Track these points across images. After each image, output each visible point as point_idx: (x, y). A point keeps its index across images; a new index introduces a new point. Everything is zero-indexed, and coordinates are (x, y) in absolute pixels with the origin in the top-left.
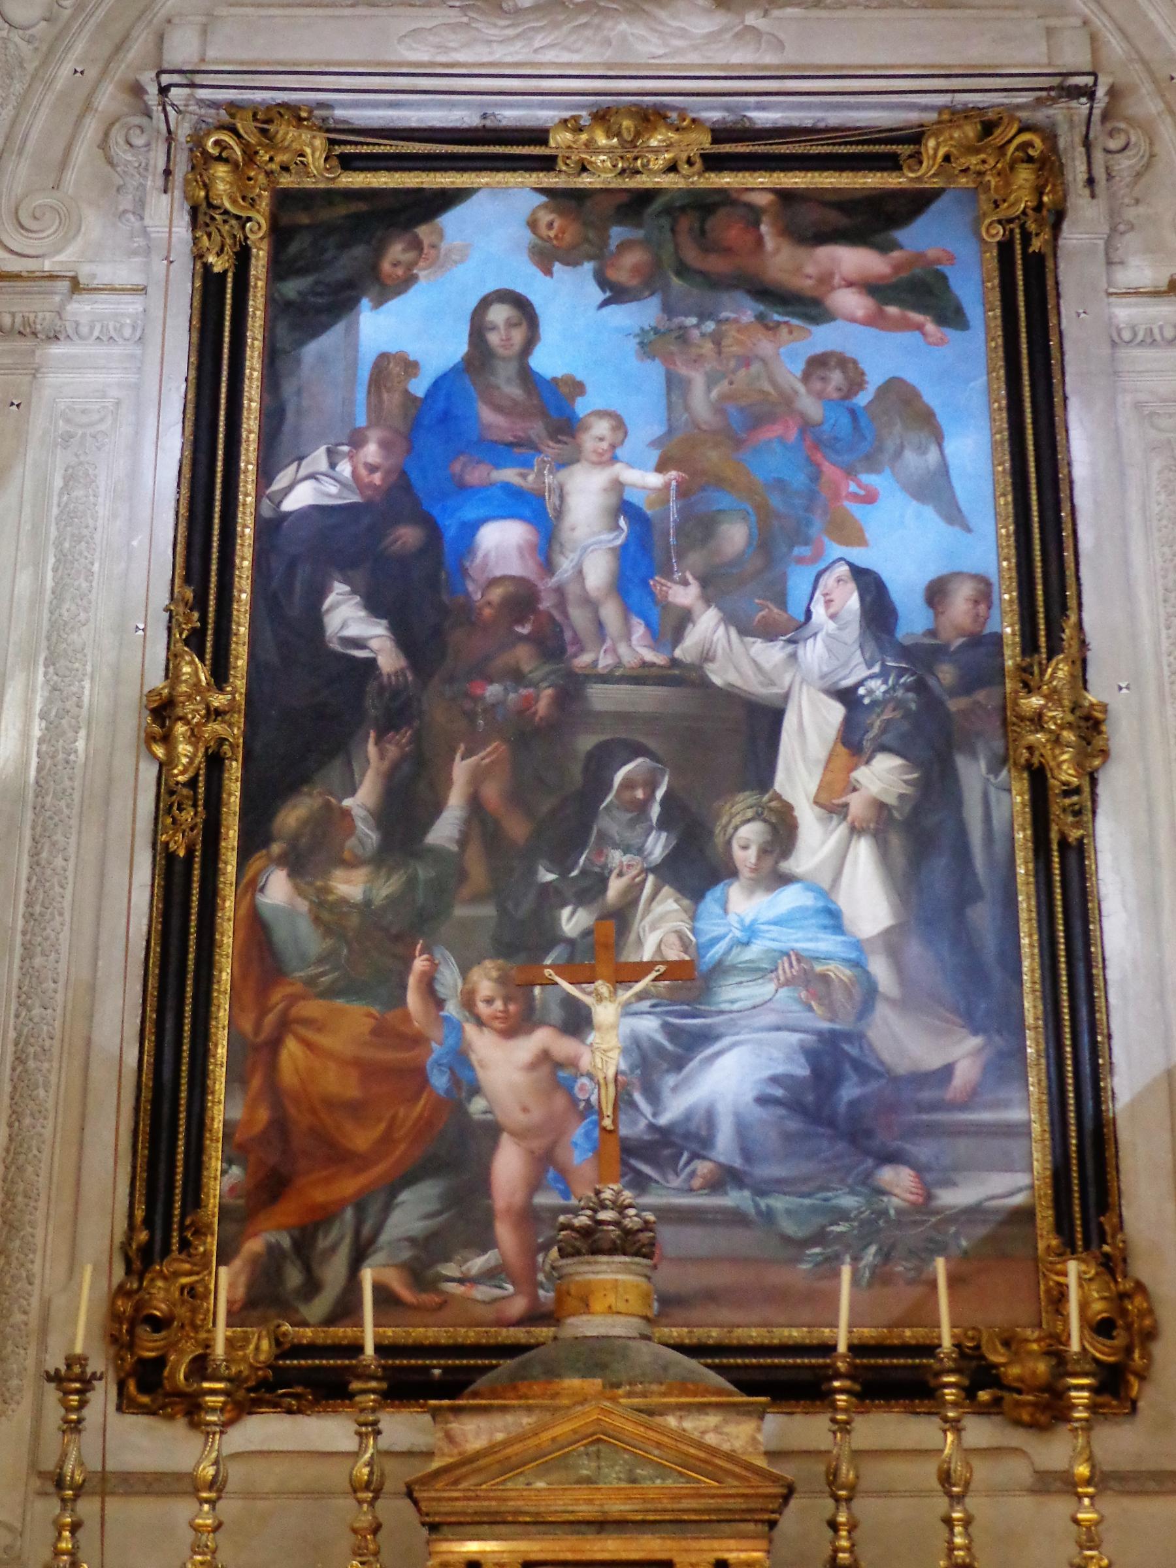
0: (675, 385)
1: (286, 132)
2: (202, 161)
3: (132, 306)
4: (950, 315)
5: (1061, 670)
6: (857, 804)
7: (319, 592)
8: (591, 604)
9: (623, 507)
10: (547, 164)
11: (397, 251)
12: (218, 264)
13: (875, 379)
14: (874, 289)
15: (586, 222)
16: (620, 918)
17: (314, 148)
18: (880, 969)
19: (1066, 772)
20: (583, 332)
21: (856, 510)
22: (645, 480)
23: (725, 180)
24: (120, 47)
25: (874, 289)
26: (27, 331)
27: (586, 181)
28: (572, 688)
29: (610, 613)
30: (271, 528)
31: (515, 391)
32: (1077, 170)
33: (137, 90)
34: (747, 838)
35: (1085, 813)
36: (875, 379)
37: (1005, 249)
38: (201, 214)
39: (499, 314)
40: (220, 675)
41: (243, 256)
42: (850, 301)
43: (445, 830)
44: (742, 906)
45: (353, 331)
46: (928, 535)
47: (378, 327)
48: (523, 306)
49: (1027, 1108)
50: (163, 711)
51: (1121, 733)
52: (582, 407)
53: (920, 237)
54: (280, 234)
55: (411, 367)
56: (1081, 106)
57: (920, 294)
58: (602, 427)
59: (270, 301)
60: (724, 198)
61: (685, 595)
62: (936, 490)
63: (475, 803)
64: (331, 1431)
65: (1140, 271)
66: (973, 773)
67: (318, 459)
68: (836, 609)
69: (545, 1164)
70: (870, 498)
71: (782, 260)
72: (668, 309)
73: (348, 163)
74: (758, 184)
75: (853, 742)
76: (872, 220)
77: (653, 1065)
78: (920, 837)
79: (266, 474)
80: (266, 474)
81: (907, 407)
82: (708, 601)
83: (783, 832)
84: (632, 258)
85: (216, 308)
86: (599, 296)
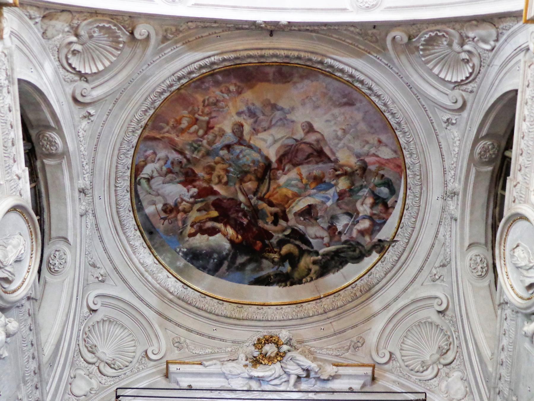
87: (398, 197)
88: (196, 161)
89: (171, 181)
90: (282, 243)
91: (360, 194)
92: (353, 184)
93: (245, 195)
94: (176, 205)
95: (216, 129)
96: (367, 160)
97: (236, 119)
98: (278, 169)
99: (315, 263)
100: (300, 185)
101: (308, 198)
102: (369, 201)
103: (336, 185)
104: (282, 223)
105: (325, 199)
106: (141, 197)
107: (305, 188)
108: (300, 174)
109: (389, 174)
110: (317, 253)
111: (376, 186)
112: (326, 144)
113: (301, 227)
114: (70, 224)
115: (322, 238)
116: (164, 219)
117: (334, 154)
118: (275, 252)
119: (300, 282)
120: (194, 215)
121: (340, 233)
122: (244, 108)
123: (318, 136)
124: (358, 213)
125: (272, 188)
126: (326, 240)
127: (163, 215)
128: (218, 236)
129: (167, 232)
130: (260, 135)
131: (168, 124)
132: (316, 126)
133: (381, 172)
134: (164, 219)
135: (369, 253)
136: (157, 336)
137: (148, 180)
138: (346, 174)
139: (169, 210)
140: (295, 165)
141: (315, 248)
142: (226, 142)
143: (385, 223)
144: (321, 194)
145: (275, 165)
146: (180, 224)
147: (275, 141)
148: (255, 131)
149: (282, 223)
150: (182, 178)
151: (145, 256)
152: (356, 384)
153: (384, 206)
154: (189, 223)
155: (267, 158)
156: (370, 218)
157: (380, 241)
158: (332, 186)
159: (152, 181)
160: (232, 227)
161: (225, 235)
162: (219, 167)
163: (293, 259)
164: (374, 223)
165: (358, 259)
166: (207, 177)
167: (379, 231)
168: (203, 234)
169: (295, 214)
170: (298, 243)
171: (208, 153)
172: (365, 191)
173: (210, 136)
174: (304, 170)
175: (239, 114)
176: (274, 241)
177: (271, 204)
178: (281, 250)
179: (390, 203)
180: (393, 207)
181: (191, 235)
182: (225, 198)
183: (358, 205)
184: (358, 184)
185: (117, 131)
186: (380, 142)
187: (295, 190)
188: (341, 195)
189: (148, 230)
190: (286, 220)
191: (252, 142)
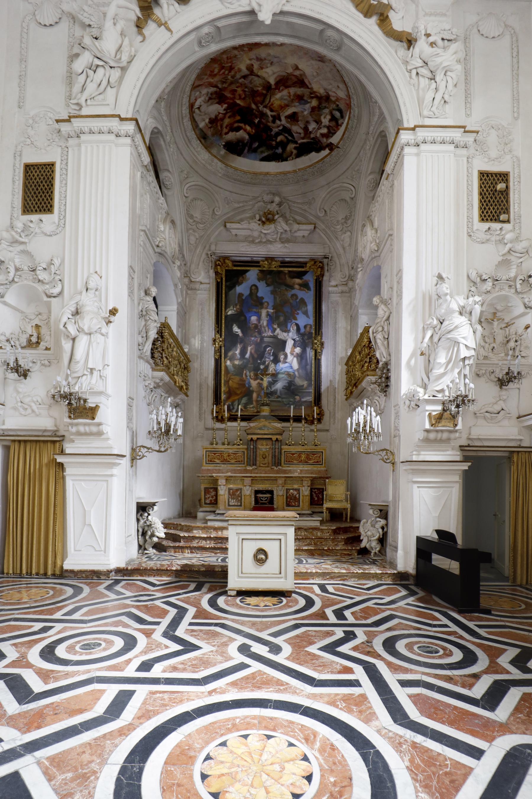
0: (275, 298)
1: (227, 261)
2: (216, 265)
4: (309, 289)
7: (232, 325)
8: (264, 327)
9: (268, 315)
10: (259, 266)
11: (241, 278)
12: (219, 280)
13: (299, 298)
14: (300, 285)
15: (265, 275)
17: (230, 264)
20: (264, 291)
21: (297, 316)
23: (282, 269)
24: (205, 247)
25: (300, 285)
26: (195, 289)
27: (264, 269)
29: (267, 328)
30: (226, 316)
31: (255, 298)
32: (326, 268)
33: (207, 254)
36: (299, 298)
37: (316, 280)
38: (217, 273)
39: (253, 288)
41: (222, 279)
42: (297, 287)
45: (235, 290)
47: (239, 289)
52: (264, 301)
54: (226, 276)
55: (243, 295)
56: (327, 260)
57: (305, 286)
58: (266, 304)
59: (226, 286)
60: (281, 271)
61: (275, 326)
62: (306, 313)
65: (333, 283)
67: (232, 308)
70: (298, 314)
71: (289, 280)
72: (274, 287)
73: (235, 266)
74: (286, 270)
76: (300, 275)
79: (225, 309)
80: (225, 309)
81: (303, 302)
82: (278, 327)
84: (270, 280)
85: (218, 286)
86: (265, 285)
87: (344, 120)
88: (225, 89)
89: (212, 104)
90: (278, 134)
91: (324, 111)
92: (320, 103)
93: (256, 104)
94: (216, 117)
95: (236, 68)
96: (330, 93)
97: (248, 62)
98: (275, 89)
99: (295, 148)
100: (289, 99)
101: (293, 108)
102: (329, 117)
103: (310, 102)
104: (278, 122)
105: (304, 110)
106: (197, 119)
107: (292, 101)
108: (289, 93)
109: (342, 106)
110: (296, 143)
111: (334, 109)
112: (306, 78)
113: (288, 125)
114: (169, 162)
115: (300, 134)
116: (210, 128)
117: (310, 84)
118: (273, 141)
119: (286, 160)
120: (227, 121)
121: (311, 132)
122: (254, 57)
123: (302, 72)
124: (322, 123)
125: (272, 100)
126: (302, 135)
127: (210, 125)
128: (241, 132)
129: (213, 135)
130: (264, 70)
131: (206, 75)
132: (300, 67)
133: (337, 103)
134: (210, 128)
135: (324, 149)
136: (217, 201)
137: (199, 108)
138: (316, 97)
139: (213, 121)
140: (287, 87)
141: (296, 139)
142: (243, 74)
143: (335, 133)
144: (302, 106)
145: (273, 87)
146: (219, 128)
147: (274, 73)
148: (262, 68)
149: (278, 122)
150: (217, 101)
151: (203, 155)
152: (306, 233)
153: (336, 123)
154: (225, 125)
155: (269, 82)
156: (328, 127)
157: (331, 143)
158: (309, 102)
159: (201, 108)
160: (249, 125)
161: (245, 130)
162: (239, 90)
163: (283, 145)
164: (329, 132)
165: (318, 150)
166: (232, 96)
167: (332, 137)
168: (232, 131)
169: (286, 117)
170: (286, 135)
171: (232, 83)
172: (327, 111)
173: (232, 73)
174: (292, 90)
175: (250, 60)
176: (273, 133)
177: (272, 110)
178: (276, 139)
179: (340, 122)
180: (341, 126)
181: (226, 133)
182: (244, 107)
183: (322, 117)
184: (324, 105)
185: (179, 94)
186: (338, 87)
187: (286, 102)
188: (313, 109)
189: (203, 137)
190: (280, 120)
191: (259, 74)
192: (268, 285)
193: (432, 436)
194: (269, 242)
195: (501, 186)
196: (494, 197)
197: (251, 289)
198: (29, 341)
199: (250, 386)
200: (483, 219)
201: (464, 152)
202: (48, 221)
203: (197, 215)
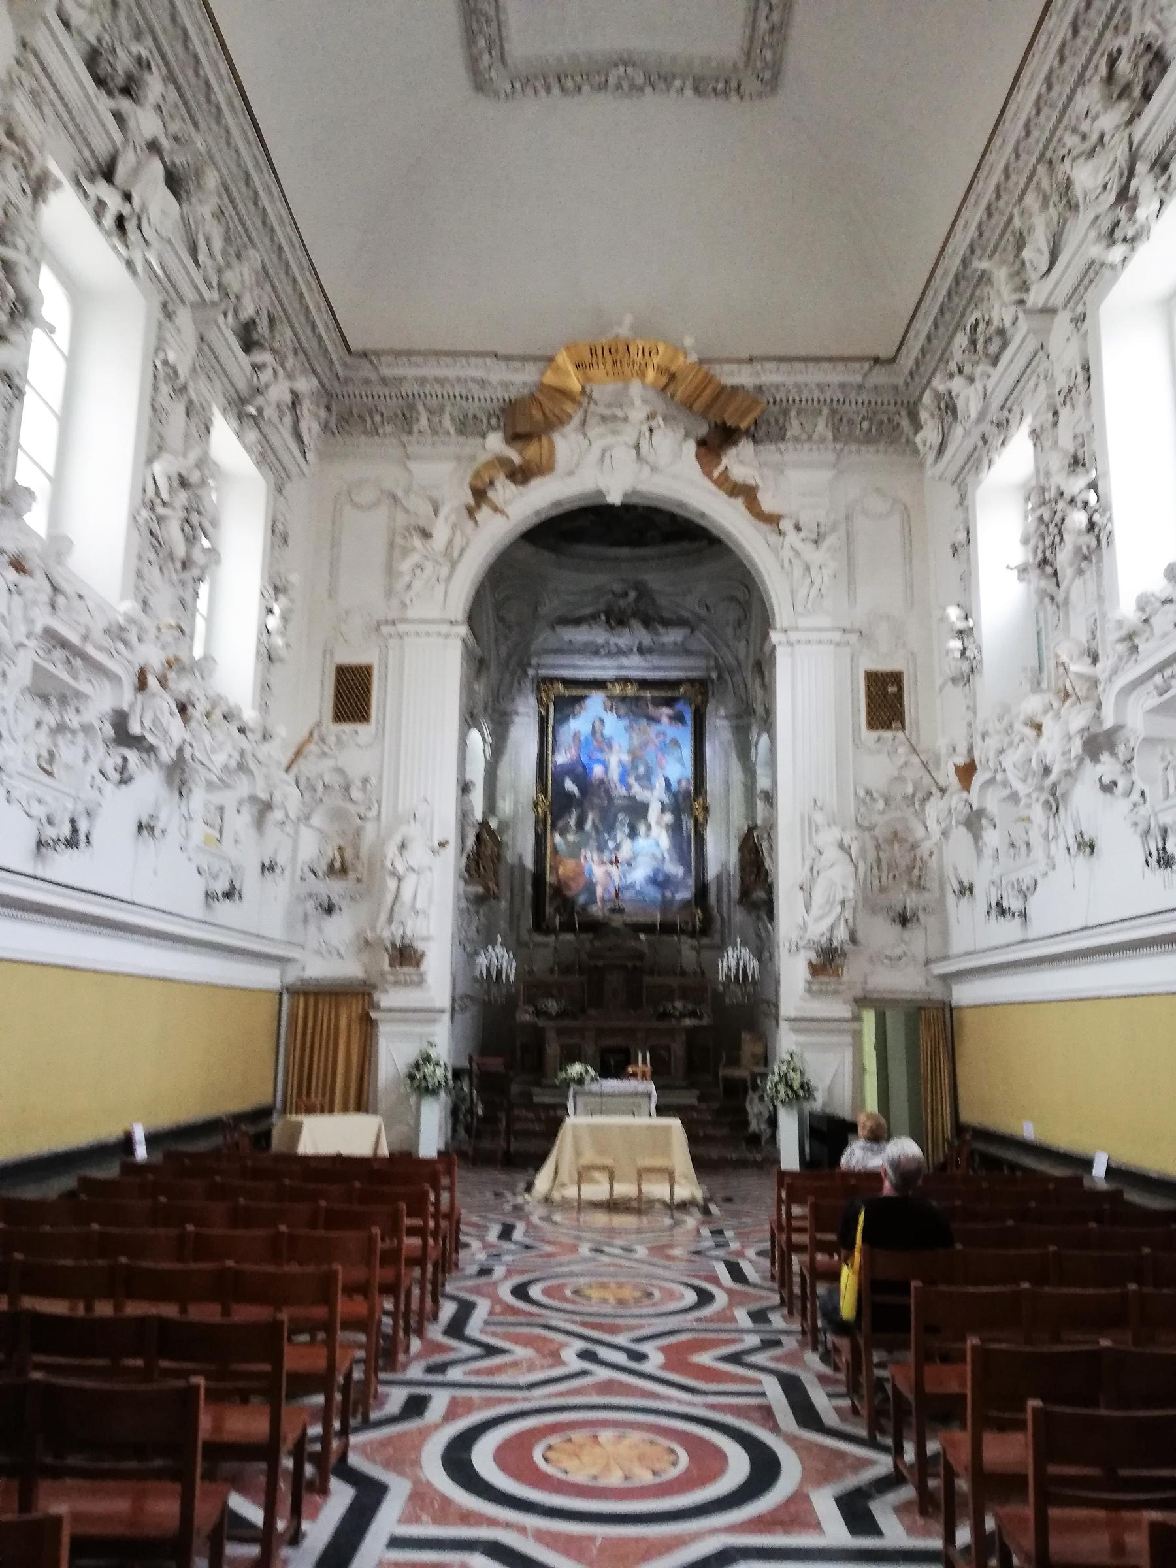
0: (631, 738)
2: (539, 689)
3: (526, 719)
5: (701, 800)
6: (663, 824)
9: (620, 762)
11: (577, 707)
16: (618, 847)
17: (561, 687)
18: (667, 856)
19: (701, 818)
20: (613, 725)
22: (626, 758)
25: (671, 718)
28: (610, 799)
29: (618, 785)
31: (600, 739)
34: (642, 829)
35: (704, 829)
38: (540, 702)
40: (546, 797)
42: (665, 720)
43: (588, 826)
44: (642, 843)
46: (678, 769)
48: (602, 721)
49: (691, 882)
50: (536, 805)
51: (711, 811)
53: (681, 706)
57: (678, 718)
62: (680, 760)
63: (593, 823)
64: (569, 937)
66: (685, 818)
68: (660, 784)
69: (606, 889)
71: (651, 710)
74: (648, 694)
75: (663, 811)
76: (669, 702)
77: (624, 875)
78: (675, 829)
83: (649, 827)
192: (619, 717)
193: (815, 987)
194: (621, 652)
195: (892, 689)
196: (885, 701)
197: (593, 727)
198: (331, 867)
199: (591, 874)
200: (871, 726)
201: (848, 650)
202: (364, 731)
203: (511, 617)
